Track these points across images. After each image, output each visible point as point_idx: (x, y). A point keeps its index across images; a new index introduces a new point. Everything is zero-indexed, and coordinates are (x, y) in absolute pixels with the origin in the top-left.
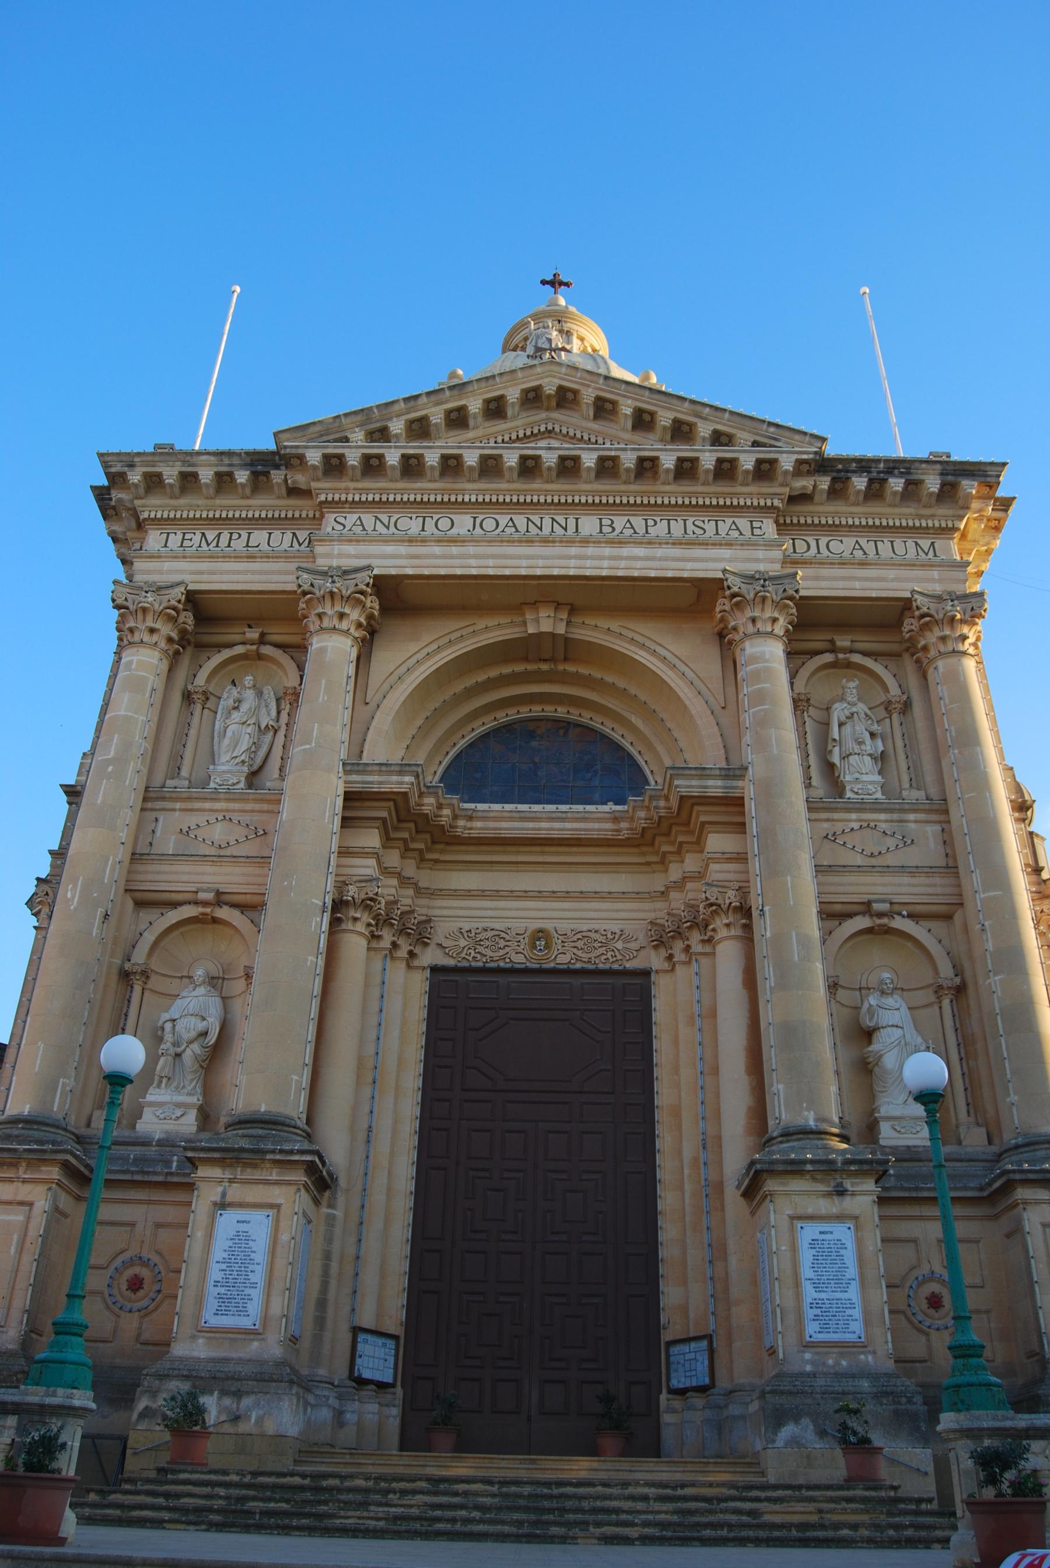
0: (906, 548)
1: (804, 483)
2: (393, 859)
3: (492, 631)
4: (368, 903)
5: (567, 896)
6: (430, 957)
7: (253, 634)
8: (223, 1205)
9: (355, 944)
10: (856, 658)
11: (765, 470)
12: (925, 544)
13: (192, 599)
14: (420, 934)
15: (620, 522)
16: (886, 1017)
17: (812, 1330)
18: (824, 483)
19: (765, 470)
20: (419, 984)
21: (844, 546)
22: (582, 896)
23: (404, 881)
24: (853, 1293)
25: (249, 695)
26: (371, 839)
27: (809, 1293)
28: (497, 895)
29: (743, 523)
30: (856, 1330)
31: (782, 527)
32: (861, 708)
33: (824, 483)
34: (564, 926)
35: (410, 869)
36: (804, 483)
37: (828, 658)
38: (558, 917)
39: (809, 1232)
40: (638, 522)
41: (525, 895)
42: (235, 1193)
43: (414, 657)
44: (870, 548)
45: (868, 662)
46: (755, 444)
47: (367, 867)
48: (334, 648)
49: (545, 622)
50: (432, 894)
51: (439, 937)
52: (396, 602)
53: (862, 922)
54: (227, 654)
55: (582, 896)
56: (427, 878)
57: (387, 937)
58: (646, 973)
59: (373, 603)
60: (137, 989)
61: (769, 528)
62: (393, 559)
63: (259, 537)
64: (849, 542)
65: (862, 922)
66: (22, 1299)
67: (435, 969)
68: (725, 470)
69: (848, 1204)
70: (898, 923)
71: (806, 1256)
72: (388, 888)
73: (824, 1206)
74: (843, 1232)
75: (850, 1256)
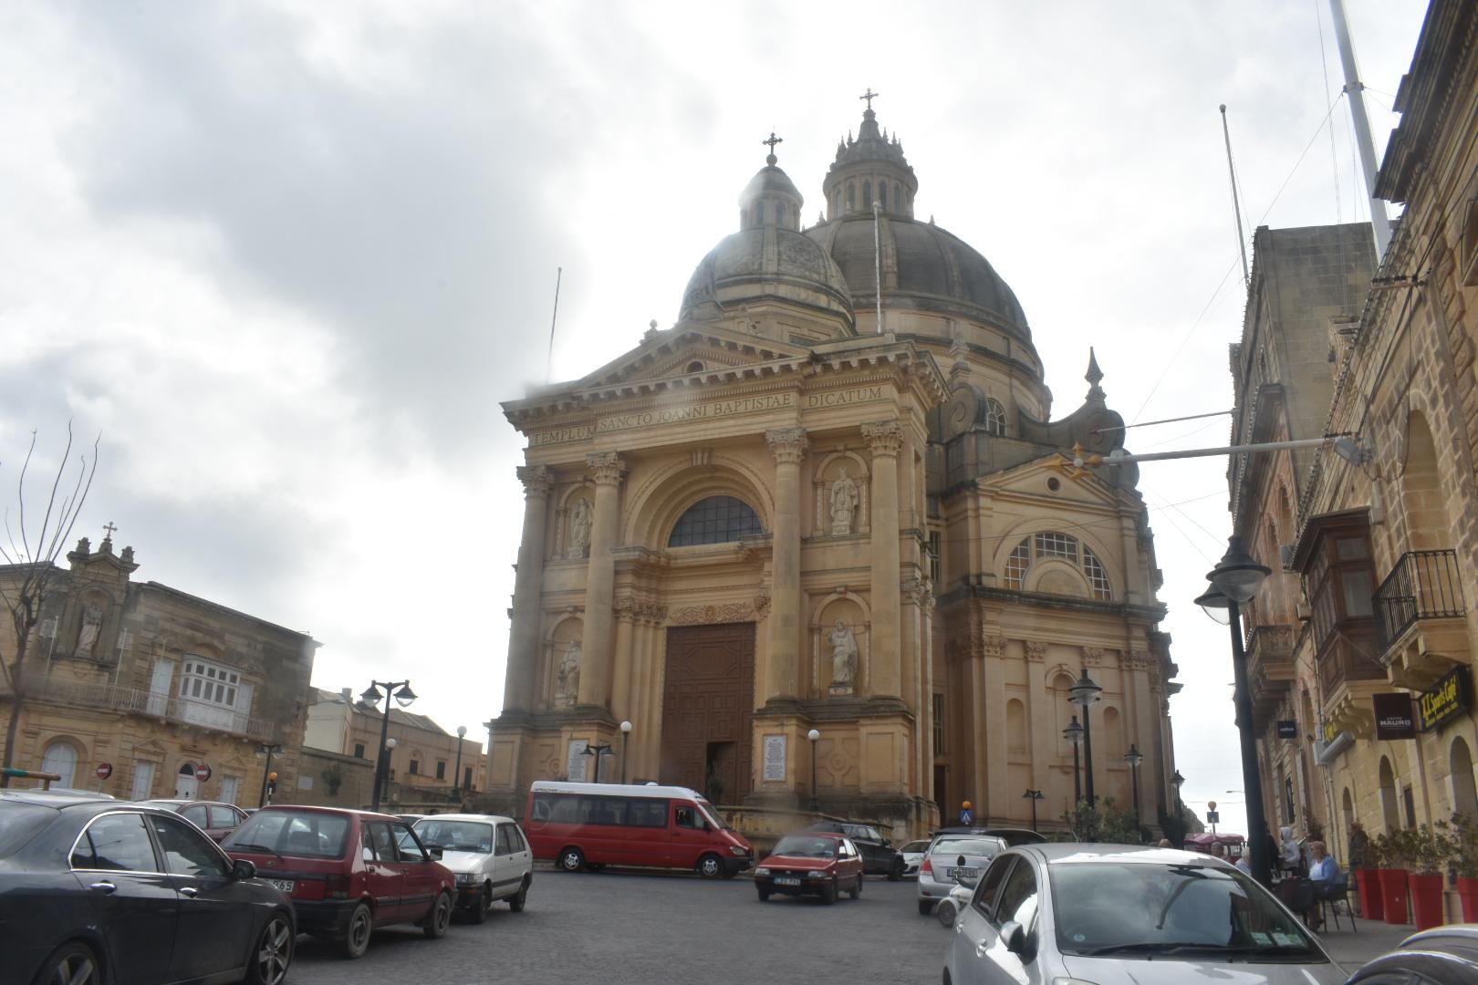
0: (865, 393)
1: (809, 370)
2: (643, 583)
3: (679, 465)
4: (629, 609)
5: (722, 589)
6: (667, 623)
7: (580, 478)
8: (572, 739)
9: (625, 628)
10: (849, 454)
11: (786, 369)
12: (875, 389)
13: (550, 468)
14: (661, 612)
15: (724, 405)
16: (838, 641)
17: (766, 777)
18: (818, 369)
19: (786, 369)
20: (662, 636)
21: (834, 398)
22: (728, 588)
23: (649, 591)
24: (782, 763)
25: (582, 509)
26: (629, 579)
27: (767, 763)
28: (692, 591)
29: (780, 397)
30: (782, 777)
31: (802, 392)
32: (849, 482)
33: (818, 369)
34: (720, 604)
35: (654, 585)
36: (809, 370)
37: (834, 455)
38: (716, 600)
39: (769, 740)
40: (732, 404)
41: (704, 590)
42: (575, 735)
43: (644, 485)
44: (847, 397)
45: (854, 456)
46: (782, 356)
47: (626, 592)
48: (603, 493)
49: (699, 460)
50: (666, 593)
51: (670, 613)
52: (631, 462)
53: (834, 597)
54: (573, 488)
55: (728, 588)
56: (663, 587)
57: (642, 620)
58: (752, 625)
59: (622, 465)
60: (548, 654)
61: (793, 398)
62: (627, 442)
63: (575, 431)
64: (837, 394)
65: (834, 597)
66: (514, 776)
67: (669, 629)
68: (767, 372)
69: (786, 730)
70: (850, 596)
71: (767, 750)
72: (643, 596)
73: (778, 730)
74: (781, 740)
75: (783, 749)
